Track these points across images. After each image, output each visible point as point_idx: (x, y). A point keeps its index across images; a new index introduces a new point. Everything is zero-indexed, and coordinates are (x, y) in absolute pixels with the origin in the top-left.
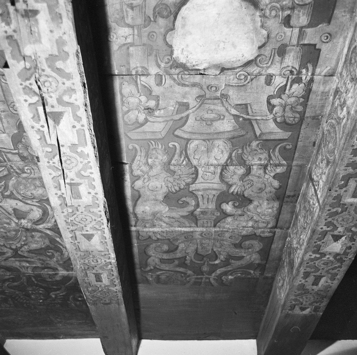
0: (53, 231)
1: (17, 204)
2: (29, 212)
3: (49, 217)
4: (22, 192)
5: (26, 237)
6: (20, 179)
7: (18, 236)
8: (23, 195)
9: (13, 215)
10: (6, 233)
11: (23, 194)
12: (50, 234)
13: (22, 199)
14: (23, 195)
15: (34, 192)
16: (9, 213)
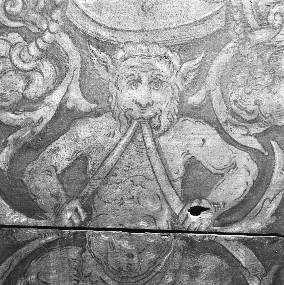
0: (254, 250)
1: (204, 140)
2: (223, 175)
3: (264, 197)
4: (233, 97)
5: (176, 272)
6: (246, 49)
7: (159, 268)
8: (233, 106)
9: (178, 184)
10: (130, 255)
11: (235, 102)
12: (243, 263)
13: (227, 122)
14: (233, 106)
15: (264, 97)
16: (168, 175)
